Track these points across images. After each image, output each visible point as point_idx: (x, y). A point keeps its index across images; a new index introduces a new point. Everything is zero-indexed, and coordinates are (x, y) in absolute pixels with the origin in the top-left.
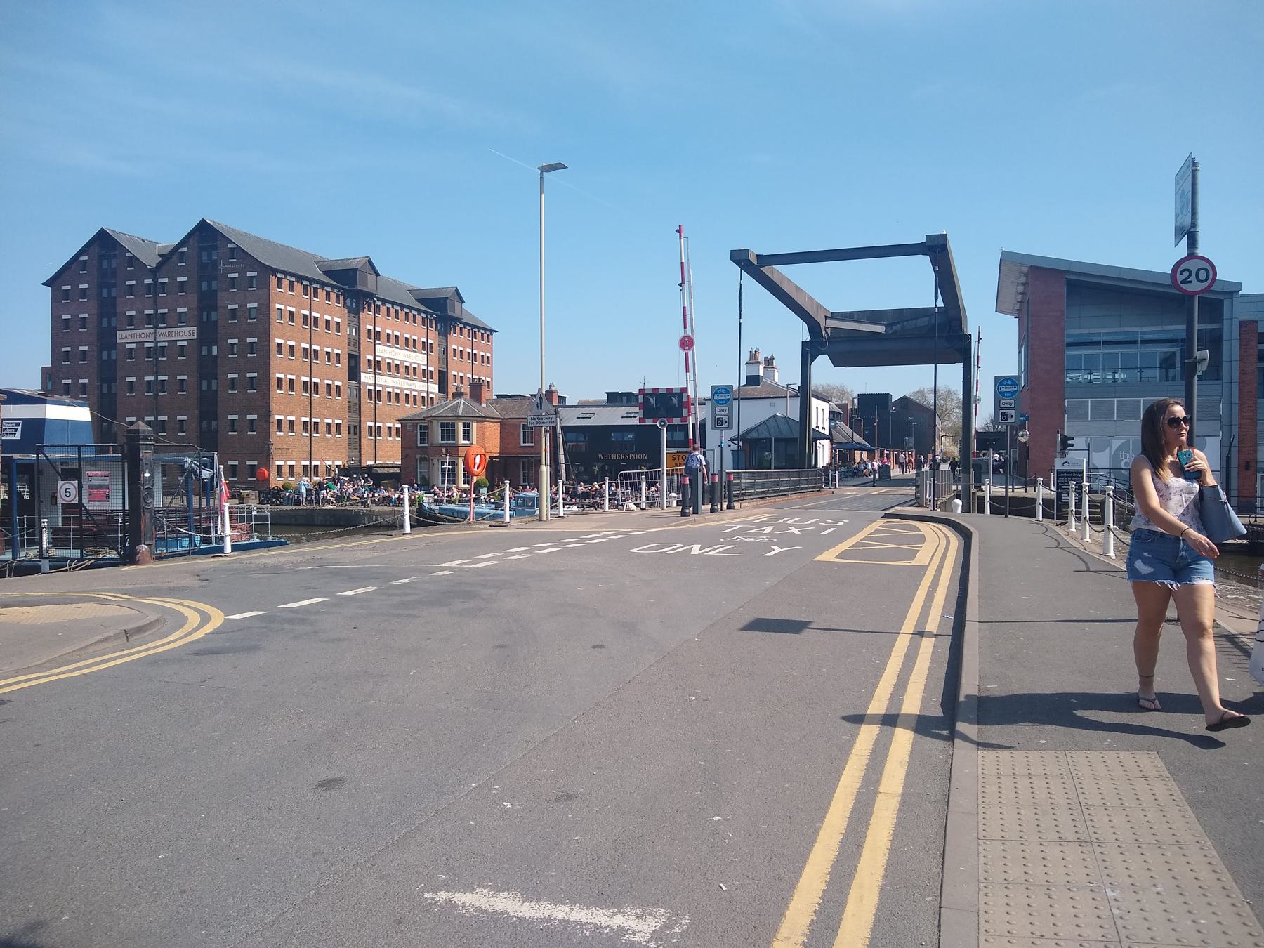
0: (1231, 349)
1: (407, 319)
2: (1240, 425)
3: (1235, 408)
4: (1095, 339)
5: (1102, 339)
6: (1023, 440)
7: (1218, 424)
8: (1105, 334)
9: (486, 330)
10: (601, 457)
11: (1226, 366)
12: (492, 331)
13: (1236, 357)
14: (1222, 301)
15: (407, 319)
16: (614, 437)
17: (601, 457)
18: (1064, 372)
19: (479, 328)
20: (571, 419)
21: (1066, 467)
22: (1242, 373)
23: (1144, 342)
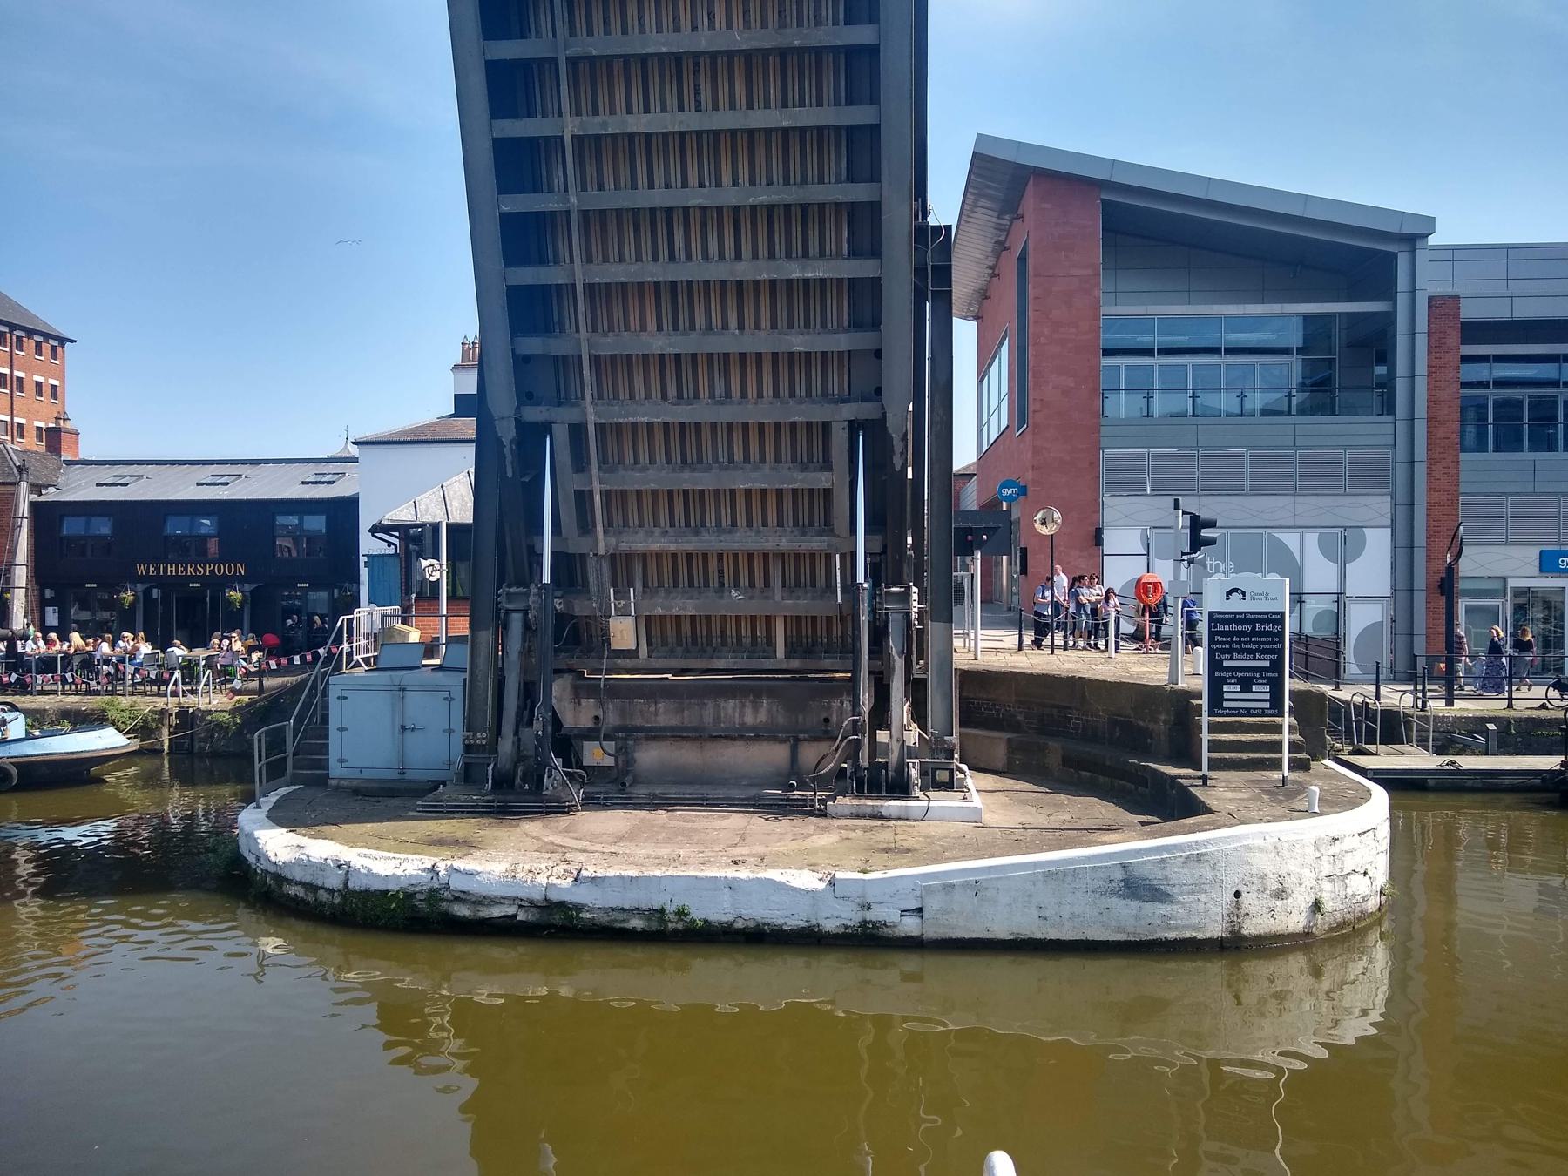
0: (1413, 355)
1: (39, 351)
2: (1430, 506)
3: (1421, 470)
4: (1144, 340)
5: (1157, 340)
6: (1045, 531)
7: (1379, 506)
8: (1169, 323)
9: (47, 336)
10: (141, 570)
11: (1401, 386)
12: (63, 341)
13: (1421, 368)
14: (1395, 255)
15: (39, 351)
16: (176, 528)
17: (141, 570)
18: (1099, 393)
19: (30, 332)
20: (79, 488)
21: (1236, 605)
22: (1433, 401)
23: (1231, 351)
